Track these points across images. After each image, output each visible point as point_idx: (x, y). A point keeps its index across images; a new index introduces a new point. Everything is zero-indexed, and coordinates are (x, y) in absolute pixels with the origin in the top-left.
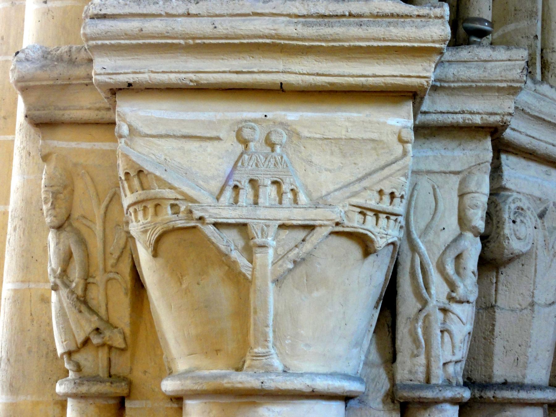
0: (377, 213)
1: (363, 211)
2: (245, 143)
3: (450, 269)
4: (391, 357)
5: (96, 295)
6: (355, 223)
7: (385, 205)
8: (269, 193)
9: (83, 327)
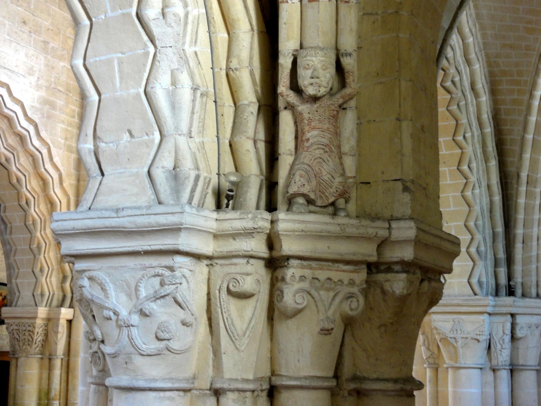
0: (480, 335)
1: (477, 335)
2: (454, 322)
3: (501, 342)
5: (431, 348)
6: (475, 337)
7: (481, 333)
8: (459, 331)
9: (429, 354)
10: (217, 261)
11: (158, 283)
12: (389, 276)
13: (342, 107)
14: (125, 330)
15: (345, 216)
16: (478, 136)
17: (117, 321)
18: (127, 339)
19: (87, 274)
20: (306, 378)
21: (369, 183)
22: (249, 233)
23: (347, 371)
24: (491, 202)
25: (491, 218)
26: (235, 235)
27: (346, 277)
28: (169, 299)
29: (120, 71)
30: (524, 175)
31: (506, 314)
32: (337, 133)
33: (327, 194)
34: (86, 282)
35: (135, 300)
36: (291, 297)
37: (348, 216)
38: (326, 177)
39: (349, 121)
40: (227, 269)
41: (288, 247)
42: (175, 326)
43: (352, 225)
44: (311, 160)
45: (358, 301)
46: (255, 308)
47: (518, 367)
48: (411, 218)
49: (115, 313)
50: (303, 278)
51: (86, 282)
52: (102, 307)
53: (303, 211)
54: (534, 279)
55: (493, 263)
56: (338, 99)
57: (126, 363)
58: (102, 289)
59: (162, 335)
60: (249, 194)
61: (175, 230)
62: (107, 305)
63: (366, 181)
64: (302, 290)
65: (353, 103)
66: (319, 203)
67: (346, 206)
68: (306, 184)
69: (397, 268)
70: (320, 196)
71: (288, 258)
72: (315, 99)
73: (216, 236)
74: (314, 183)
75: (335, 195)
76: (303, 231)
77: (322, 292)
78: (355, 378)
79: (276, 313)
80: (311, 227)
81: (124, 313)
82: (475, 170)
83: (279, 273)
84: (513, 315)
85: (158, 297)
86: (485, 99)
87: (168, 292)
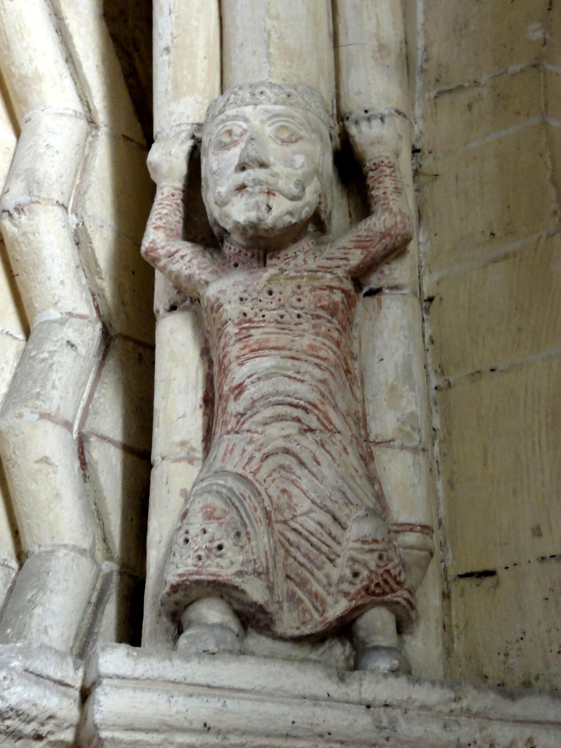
13: (361, 282)
15: (394, 672)
32: (348, 369)
33: (316, 587)
37: (404, 670)
43: (423, 707)
44: (251, 458)
53: (212, 647)
60: (38, 611)
63: (479, 569)
65: (399, 272)
66: (288, 622)
67: (402, 642)
68: (227, 543)
70: (292, 596)
72: (264, 245)
74: (262, 541)
75: (352, 590)
76: (206, 728)
80: (241, 711)
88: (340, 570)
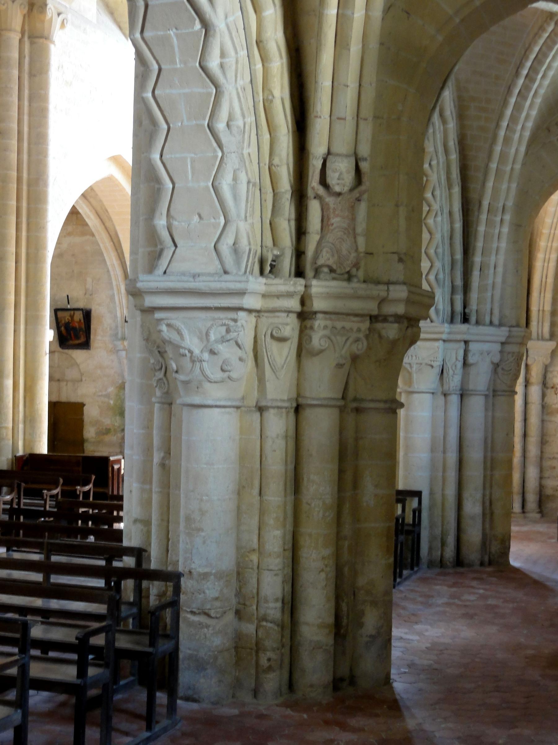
3: (454, 368)
4: (442, 385)
6: (430, 363)
8: (414, 358)
10: (262, 314)
11: (225, 330)
12: (385, 325)
13: (358, 200)
14: (198, 364)
16: (443, 163)
17: (191, 357)
18: (199, 370)
19: (166, 322)
20: (325, 399)
21: (372, 254)
22: (289, 295)
23: (351, 394)
24: (452, 230)
25: (451, 245)
26: (279, 296)
27: (355, 326)
28: (232, 343)
29: (192, 168)
30: (485, 204)
31: (459, 341)
32: (353, 219)
34: (164, 328)
35: (205, 343)
36: (317, 340)
37: (359, 281)
38: (344, 252)
39: (362, 209)
40: (271, 320)
41: (318, 305)
42: (234, 361)
45: (363, 344)
46: (290, 349)
47: (468, 392)
48: (404, 283)
49: (190, 352)
50: (325, 327)
51: (164, 328)
52: (177, 347)
54: (488, 307)
55: (451, 289)
56: (356, 194)
57: (198, 388)
58: (178, 333)
59: (225, 367)
61: (242, 293)
62: (183, 345)
64: (325, 336)
65: (365, 196)
66: (339, 271)
69: (391, 319)
71: (315, 313)
72: (339, 194)
73: (264, 296)
77: (339, 338)
78: (355, 400)
79: (304, 352)
81: (197, 351)
82: (438, 198)
83: (308, 323)
84: (466, 342)
85: (223, 340)
86: (452, 125)
87: (232, 337)
88: (349, 262)
